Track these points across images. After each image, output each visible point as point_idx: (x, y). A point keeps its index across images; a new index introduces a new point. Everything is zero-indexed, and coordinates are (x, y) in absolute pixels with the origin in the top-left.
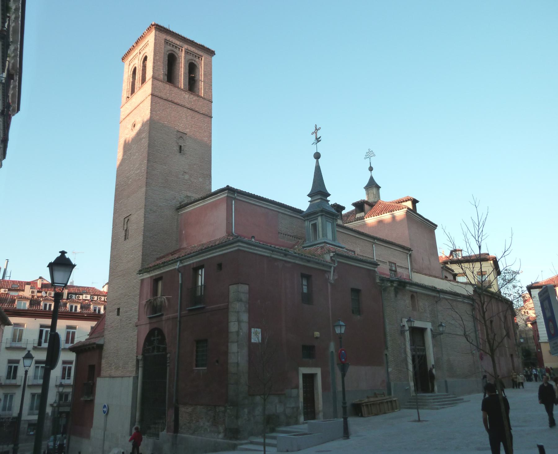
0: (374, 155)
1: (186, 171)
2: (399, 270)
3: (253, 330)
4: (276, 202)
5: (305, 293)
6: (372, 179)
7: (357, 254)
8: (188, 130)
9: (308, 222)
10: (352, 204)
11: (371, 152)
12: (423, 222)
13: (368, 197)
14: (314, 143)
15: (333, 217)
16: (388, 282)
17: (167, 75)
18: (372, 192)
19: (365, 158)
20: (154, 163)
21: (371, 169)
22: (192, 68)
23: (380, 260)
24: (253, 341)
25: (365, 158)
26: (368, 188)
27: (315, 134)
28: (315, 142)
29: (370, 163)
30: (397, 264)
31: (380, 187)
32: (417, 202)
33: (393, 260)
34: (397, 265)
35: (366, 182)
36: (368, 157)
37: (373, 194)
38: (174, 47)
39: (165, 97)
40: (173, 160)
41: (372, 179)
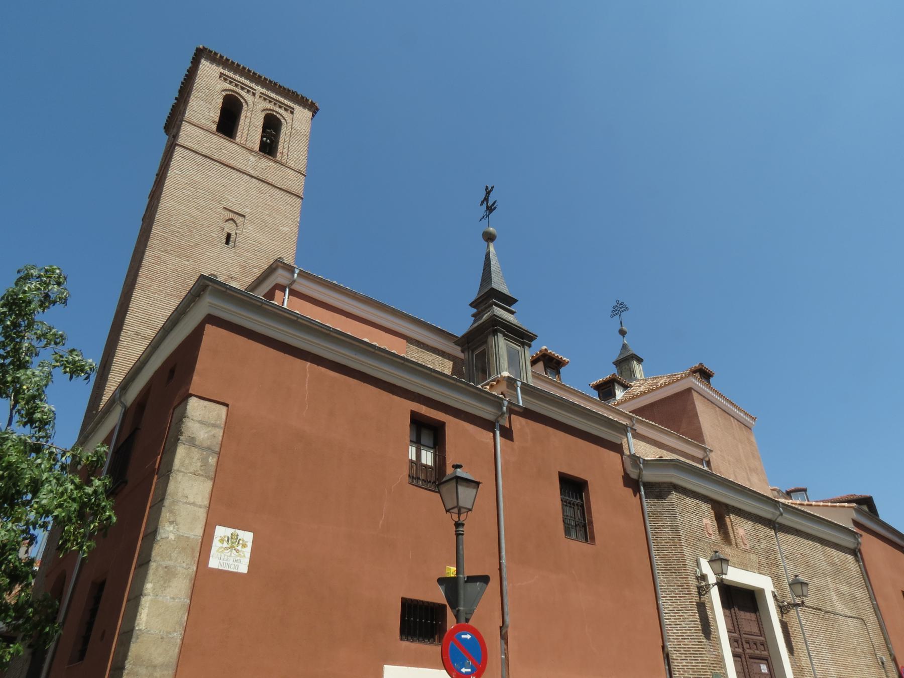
0: (627, 309)
1: (237, 276)
3: (221, 531)
5: (426, 466)
6: (624, 347)
8: (248, 210)
9: (471, 352)
11: (620, 305)
14: (483, 217)
17: (218, 123)
18: (627, 367)
19: (612, 316)
20: (162, 252)
21: (623, 333)
22: (272, 125)
24: (214, 563)
25: (612, 316)
26: (620, 363)
27: (485, 203)
28: (485, 214)
29: (621, 322)
36: (617, 314)
38: (239, 87)
39: (205, 152)
40: (208, 254)
41: (624, 347)
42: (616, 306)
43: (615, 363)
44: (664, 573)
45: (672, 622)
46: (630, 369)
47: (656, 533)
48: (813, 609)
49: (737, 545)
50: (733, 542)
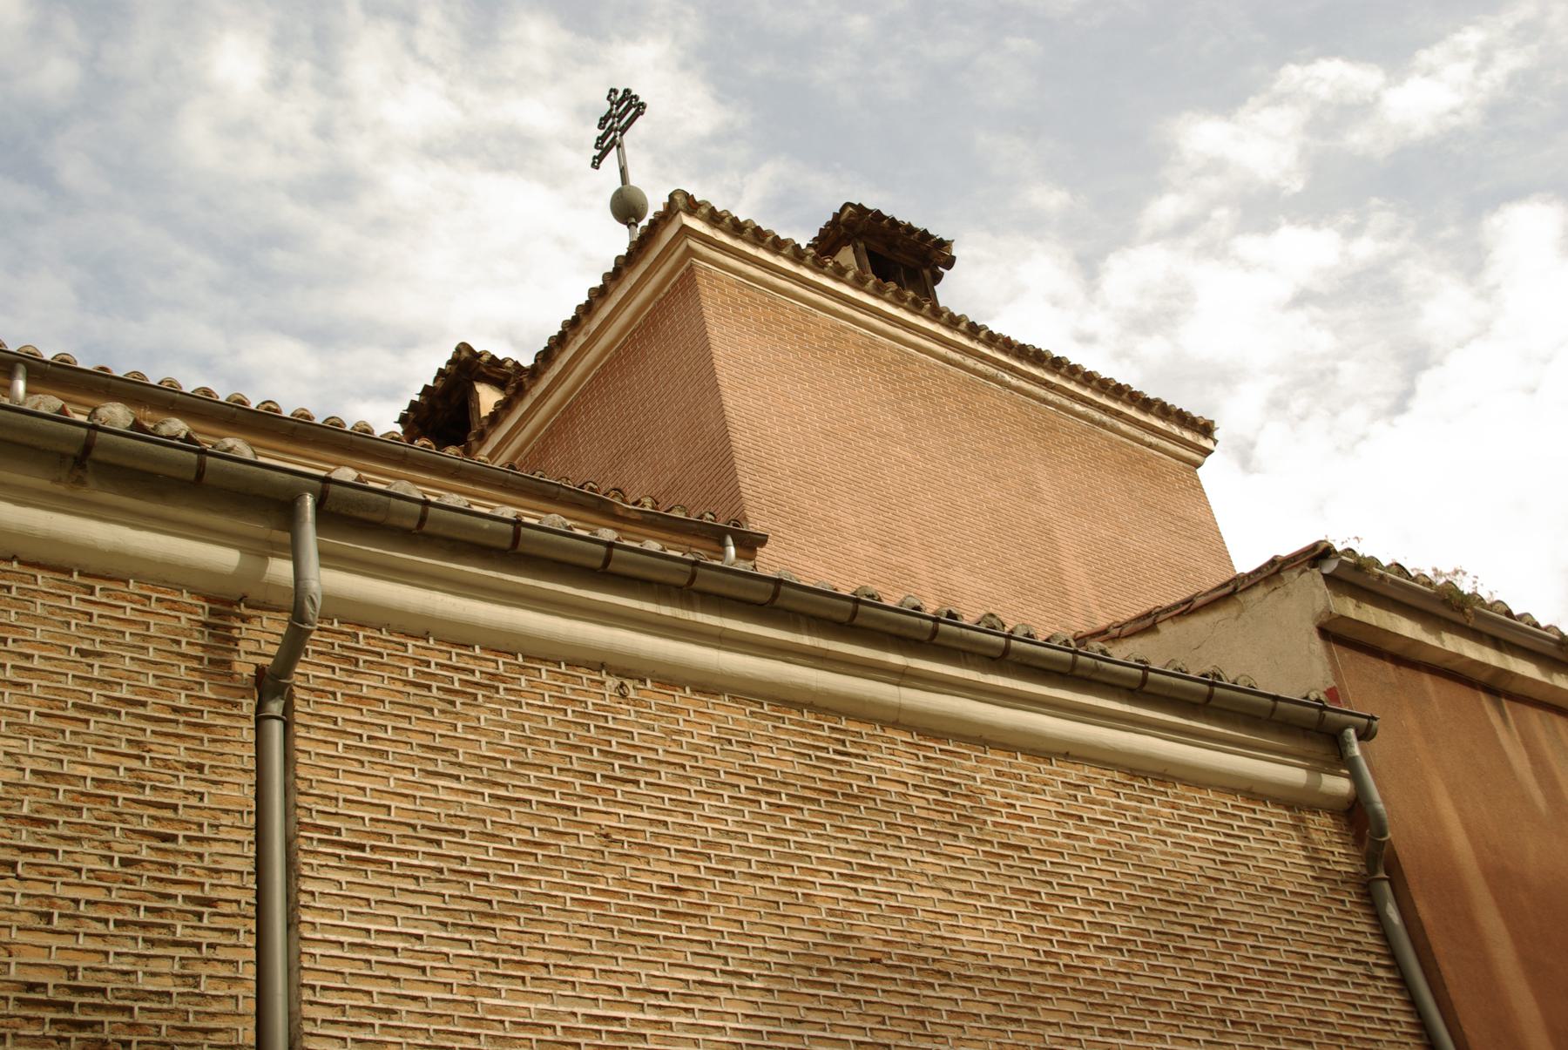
0: (640, 108)
12: (992, 370)
25: (597, 163)
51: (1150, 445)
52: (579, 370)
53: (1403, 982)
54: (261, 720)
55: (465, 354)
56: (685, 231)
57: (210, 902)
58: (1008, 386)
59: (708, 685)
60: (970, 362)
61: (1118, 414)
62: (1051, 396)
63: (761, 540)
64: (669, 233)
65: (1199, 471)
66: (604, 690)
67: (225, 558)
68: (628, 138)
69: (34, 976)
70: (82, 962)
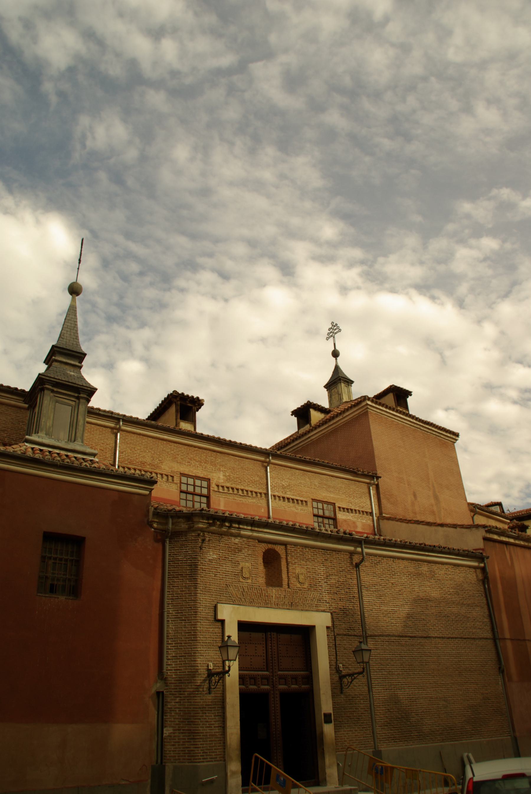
0: (340, 330)
2: (341, 516)
4: (246, 445)
7: (218, 486)
10: (291, 413)
11: (334, 326)
12: (419, 427)
13: (330, 402)
15: (76, 395)
16: (180, 520)
18: (336, 391)
19: (327, 339)
21: (335, 354)
23: (286, 496)
25: (327, 339)
26: (330, 386)
29: (335, 344)
30: (337, 505)
31: (352, 382)
32: (408, 393)
33: (323, 495)
34: (339, 508)
35: (327, 377)
36: (331, 336)
37: (338, 394)
41: (337, 369)
42: (331, 328)
43: (325, 387)
44: (174, 621)
45: (173, 667)
46: (338, 391)
47: (174, 582)
48: (396, 636)
49: (288, 585)
50: (285, 582)
51: (446, 439)
52: (339, 423)
53: (486, 596)
54: (356, 571)
55: (309, 403)
56: (367, 404)
57: (354, 597)
58: (422, 429)
59: (403, 559)
60: (415, 425)
61: (441, 434)
62: (429, 431)
63: (380, 477)
64: (364, 404)
65: (455, 444)
66: (390, 561)
67: (352, 548)
68: (336, 336)
69: (341, 607)
70: (344, 605)
